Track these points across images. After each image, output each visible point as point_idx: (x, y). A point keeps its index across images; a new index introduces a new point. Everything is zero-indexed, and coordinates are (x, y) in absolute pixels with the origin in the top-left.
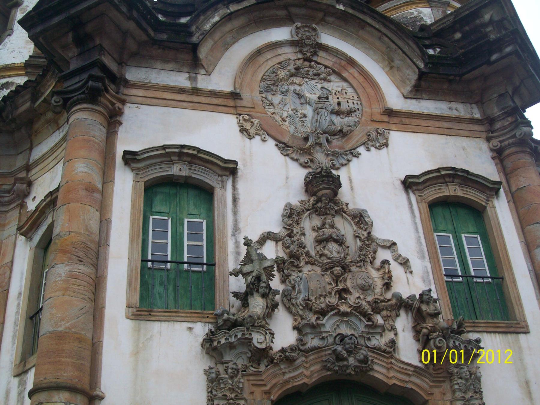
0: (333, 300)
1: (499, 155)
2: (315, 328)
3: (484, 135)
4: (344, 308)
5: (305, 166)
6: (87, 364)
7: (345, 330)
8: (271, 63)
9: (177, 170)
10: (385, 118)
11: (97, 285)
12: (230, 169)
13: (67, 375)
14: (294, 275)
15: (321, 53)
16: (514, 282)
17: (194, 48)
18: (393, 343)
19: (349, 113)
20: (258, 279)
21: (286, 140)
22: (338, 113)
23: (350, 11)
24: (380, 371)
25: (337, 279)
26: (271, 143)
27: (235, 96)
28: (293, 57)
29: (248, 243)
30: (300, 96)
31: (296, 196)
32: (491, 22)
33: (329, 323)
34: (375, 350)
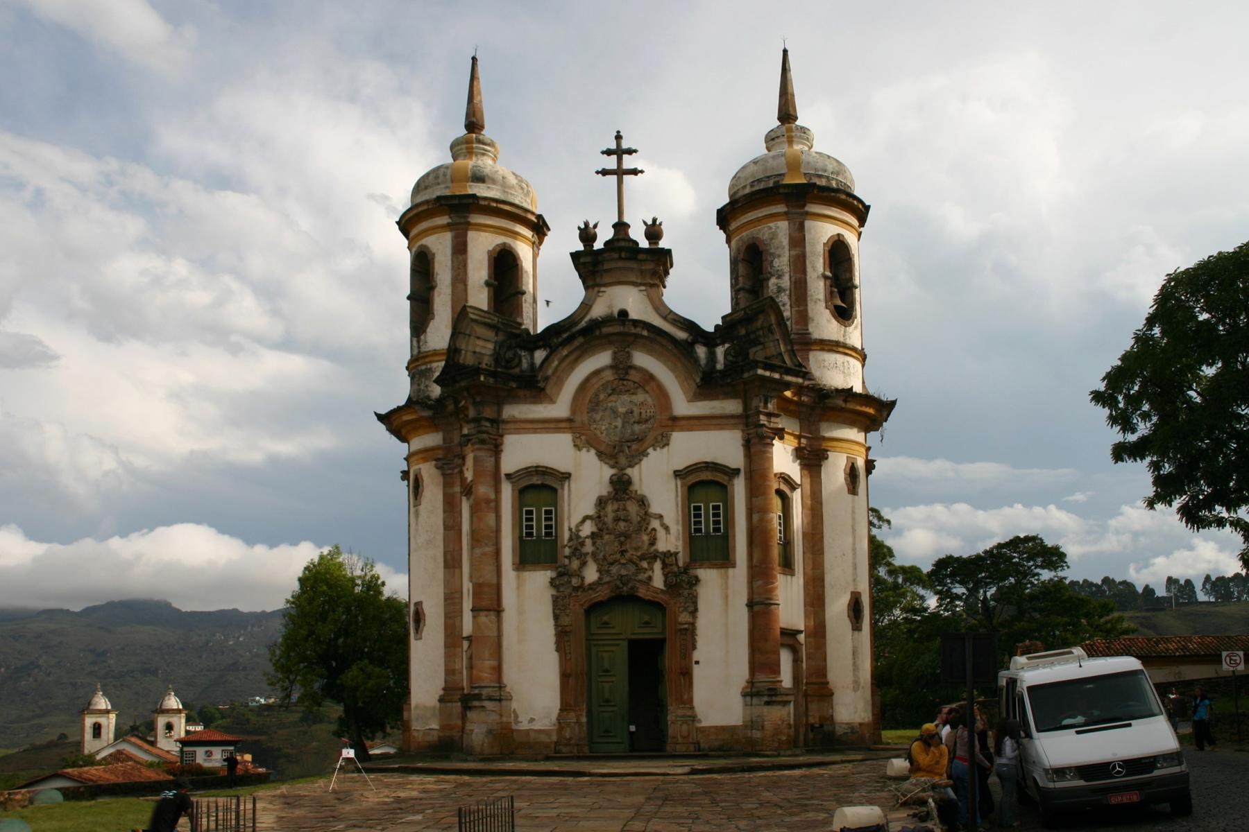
0: (618, 556)
1: (747, 445)
2: (608, 572)
3: (741, 426)
4: (623, 561)
5: (612, 467)
6: (495, 597)
7: (624, 572)
8: (596, 386)
9: (536, 480)
10: (670, 423)
11: (497, 554)
12: (567, 476)
13: (485, 603)
14: (599, 541)
15: (632, 372)
16: (734, 536)
17: (543, 389)
18: (650, 578)
19: (646, 421)
20: (576, 549)
21: (602, 449)
22: (639, 423)
23: (653, 336)
24: (642, 592)
25: (622, 544)
26: (593, 452)
27: (569, 420)
28: (610, 378)
29: (570, 529)
30: (614, 411)
31: (604, 489)
32: (762, 328)
33: (614, 569)
34: (640, 581)
